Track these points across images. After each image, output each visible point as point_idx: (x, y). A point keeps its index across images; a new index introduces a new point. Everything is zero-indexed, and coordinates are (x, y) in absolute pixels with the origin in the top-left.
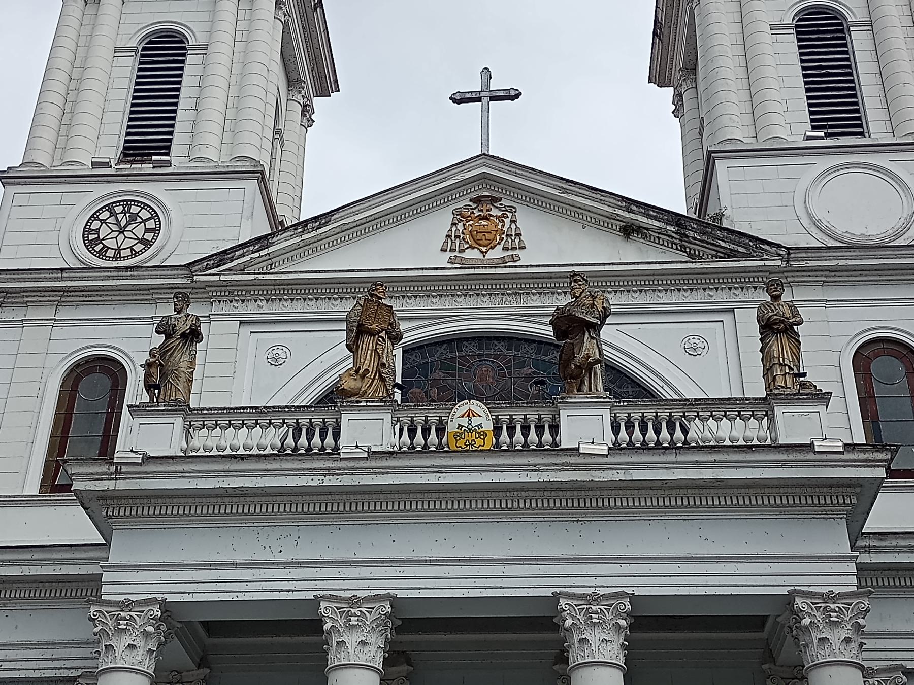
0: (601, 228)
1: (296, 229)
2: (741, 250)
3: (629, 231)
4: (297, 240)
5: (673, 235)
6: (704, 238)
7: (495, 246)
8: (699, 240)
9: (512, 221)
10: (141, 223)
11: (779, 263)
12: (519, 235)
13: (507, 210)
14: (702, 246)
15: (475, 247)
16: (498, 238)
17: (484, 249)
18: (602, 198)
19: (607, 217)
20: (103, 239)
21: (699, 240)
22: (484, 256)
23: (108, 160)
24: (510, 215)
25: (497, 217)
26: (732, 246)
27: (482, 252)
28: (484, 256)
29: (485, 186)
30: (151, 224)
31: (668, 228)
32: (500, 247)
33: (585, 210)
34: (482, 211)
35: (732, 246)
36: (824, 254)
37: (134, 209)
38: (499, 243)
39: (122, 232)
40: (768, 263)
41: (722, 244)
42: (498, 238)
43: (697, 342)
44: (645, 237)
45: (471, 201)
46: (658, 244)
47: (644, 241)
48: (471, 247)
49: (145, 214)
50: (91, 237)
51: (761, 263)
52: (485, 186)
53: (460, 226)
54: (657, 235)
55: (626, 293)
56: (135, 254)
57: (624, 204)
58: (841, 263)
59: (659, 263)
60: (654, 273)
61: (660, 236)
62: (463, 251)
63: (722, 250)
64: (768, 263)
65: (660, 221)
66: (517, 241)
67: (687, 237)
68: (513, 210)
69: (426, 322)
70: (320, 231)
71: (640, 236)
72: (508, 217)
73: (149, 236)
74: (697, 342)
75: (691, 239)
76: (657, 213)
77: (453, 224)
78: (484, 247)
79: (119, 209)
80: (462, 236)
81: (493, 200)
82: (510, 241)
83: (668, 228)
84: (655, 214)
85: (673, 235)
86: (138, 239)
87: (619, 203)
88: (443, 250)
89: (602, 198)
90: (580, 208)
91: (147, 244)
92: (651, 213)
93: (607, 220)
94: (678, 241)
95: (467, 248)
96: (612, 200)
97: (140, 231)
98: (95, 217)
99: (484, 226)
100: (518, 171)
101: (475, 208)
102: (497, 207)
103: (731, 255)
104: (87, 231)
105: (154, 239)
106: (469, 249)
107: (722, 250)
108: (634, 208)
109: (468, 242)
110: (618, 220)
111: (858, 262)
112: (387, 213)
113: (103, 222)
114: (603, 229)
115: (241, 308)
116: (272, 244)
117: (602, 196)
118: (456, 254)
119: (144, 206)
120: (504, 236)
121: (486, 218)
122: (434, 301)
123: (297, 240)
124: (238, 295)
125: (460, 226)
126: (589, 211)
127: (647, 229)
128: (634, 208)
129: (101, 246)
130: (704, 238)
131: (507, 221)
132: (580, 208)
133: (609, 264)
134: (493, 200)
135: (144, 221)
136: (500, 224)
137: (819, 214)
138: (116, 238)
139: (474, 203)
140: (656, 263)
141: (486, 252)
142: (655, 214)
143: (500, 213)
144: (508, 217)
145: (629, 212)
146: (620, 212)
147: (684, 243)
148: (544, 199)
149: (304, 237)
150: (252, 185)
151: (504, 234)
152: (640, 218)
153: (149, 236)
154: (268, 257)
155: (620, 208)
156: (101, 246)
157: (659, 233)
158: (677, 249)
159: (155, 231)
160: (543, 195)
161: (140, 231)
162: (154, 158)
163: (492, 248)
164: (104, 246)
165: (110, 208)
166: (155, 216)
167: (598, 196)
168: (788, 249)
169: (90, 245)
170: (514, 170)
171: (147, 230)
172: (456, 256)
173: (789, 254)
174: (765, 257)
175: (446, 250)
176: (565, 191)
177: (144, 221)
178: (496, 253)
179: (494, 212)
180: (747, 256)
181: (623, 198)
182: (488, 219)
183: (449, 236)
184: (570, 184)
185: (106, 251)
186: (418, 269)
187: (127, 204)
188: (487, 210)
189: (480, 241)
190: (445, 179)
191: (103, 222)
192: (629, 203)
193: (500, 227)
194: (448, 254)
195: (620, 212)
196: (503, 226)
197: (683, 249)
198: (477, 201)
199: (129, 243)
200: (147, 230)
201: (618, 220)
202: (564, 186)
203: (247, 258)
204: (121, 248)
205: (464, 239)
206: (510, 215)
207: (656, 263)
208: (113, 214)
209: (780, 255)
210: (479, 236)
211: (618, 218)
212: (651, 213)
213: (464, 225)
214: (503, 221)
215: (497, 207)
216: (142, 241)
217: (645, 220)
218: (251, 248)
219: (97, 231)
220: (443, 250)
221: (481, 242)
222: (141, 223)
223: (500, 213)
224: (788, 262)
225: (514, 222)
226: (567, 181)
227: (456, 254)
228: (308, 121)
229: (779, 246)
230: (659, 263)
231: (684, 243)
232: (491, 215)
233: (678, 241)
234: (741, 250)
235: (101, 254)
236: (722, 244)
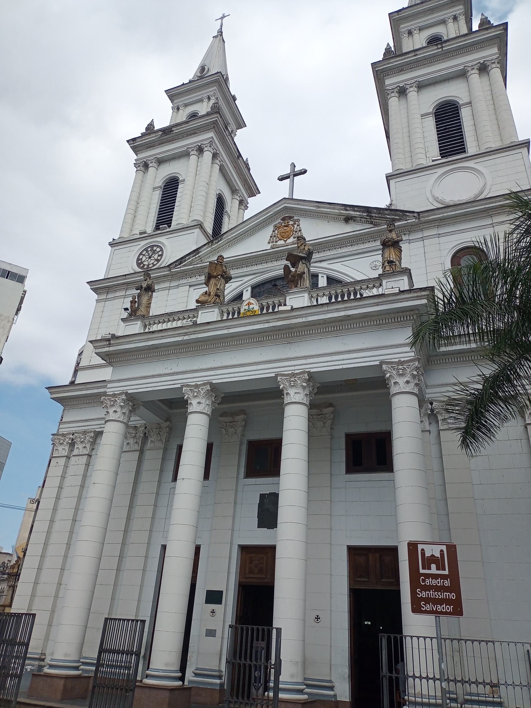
0: (336, 221)
1: (209, 244)
2: (397, 217)
3: (348, 220)
5: (367, 217)
6: (380, 216)
7: (290, 237)
8: (378, 217)
9: (298, 225)
10: (156, 253)
11: (414, 220)
12: (300, 231)
13: (296, 221)
14: (380, 220)
15: (282, 239)
16: (292, 233)
17: (285, 239)
18: (334, 207)
19: (338, 215)
20: (143, 262)
21: (378, 217)
22: (285, 242)
23: (145, 231)
24: (297, 223)
25: (292, 225)
26: (392, 217)
27: (284, 241)
28: (285, 242)
29: (287, 212)
30: (160, 253)
31: (364, 214)
32: (292, 237)
33: (329, 214)
34: (285, 223)
35: (392, 217)
36: (437, 212)
37: (155, 248)
38: (292, 236)
39: (150, 258)
40: (409, 221)
41: (388, 216)
42: (292, 233)
43: (375, 263)
44: (354, 221)
45: (281, 220)
46: (361, 223)
47: (354, 223)
48: (280, 240)
49: (158, 250)
50: (139, 262)
51: (406, 222)
52: (287, 212)
53: (276, 232)
54: (360, 219)
55: (345, 247)
57: (344, 207)
58: (445, 215)
59: (358, 231)
60: (357, 236)
61: (361, 219)
62: (276, 242)
63: (389, 220)
64: (409, 221)
65: (359, 212)
66: (299, 233)
67: (372, 217)
68: (298, 220)
69: (260, 274)
70: (218, 244)
71: (352, 221)
72: (296, 224)
73: (159, 258)
74: (375, 263)
75: (374, 217)
76: (358, 208)
77: (273, 231)
78: (285, 238)
80: (277, 235)
81: (290, 218)
82: (296, 234)
83: (364, 214)
84: (357, 209)
85: (367, 217)
86: (155, 259)
87: (342, 208)
88: (269, 243)
89: (334, 207)
90: (326, 214)
91: (158, 261)
92: (356, 209)
93: (338, 216)
94: (369, 220)
95: (278, 240)
96: (338, 207)
98: (141, 254)
99: (285, 229)
100: (298, 203)
101: (283, 223)
102: (292, 221)
104: (138, 259)
106: (280, 241)
107: (389, 220)
108: (348, 208)
109: (279, 238)
110: (343, 216)
111: (454, 213)
112: (246, 232)
113: (144, 255)
114: (337, 221)
115: (190, 280)
116: (200, 252)
117: (334, 206)
118: (274, 243)
120: (294, 232)
122: (264, 265)
123: (210, 249)
124: (189, 275)
125: (276, 232)
126: (330, 214)
127: (355, 217)
128: (348, 208)
129: (142, 264)
130: (380, 216)
131: (296, 226)
132: (326, 214)
133: (336, 235)
134: (290, 218)
135: (158, 252)
136: (293, 228)
137: (437, 195)
138: (148, 261)
139: (283, 220)
140: (357, 231)
141: (286, 241)
142: (357, 209)
143: (292, 223)
144: (296, 224)
145: (346, 211)
146: (342, 212)
147: (372, 220)
148: (311, 213)
149: (212, 247)
150: (197, 231)
151: (294, 231)
152: (351, 212)
153: (159, 258)
154: (199, 258)
155: (342, 210)
156: (142, 264)
157: (361, 218)
158: (369, 223)
159: (161, 256)
160: (310, 211)
161: (156, 256)
162: (160, 226)
163: (289, 238)
164: (144, 264)
165: (146, 250)
166: (162, 250)
167: (333, 206)
168: (418, 213)
170: (297, 202)
171: (159, 256)
172: (274, 245)
173: (419, 215)
174: (408, 218)
175: (270, 243)
176: (318, 207)
177: (158, 252)
179: (291, 223)
181: (342, 204)
182: (288, 226)
183: (271, 237)
184: (320, 203)
185: (144, 266)
186: (255, 252)
187: (152, 246)
188: (287, 223)
189: (285, 236)
190: (269, 213)
191: (144, 255)
192: (345, 207)
193: (292, 229)
194: (271, 244)
195: (342, 212)
196: (294, 228)
197: (372, 223)
198: (283, 219)
199: (152, 261)
200: (159, 256)
201: (343, 216)
202: (318, 205)
203: (191, 259)
204: (150, 264)
205: (277, 237)
206: (297, 223)
207: (357, 231)
208: (147, 251)
209: (415, 216)
210: (283, 234)
211: (342, 215)
212: (356, 209)
213: (278, 230)
214: (294, 226)
215: (292, 221)
217: (353, 213)
218: (192, 255)
219: (141, 259)
220: (269, 243)
221: (284, 237)
222: (156, 253)
223: (292, 223)
224: (419, 219)
226: (319, 202)
227: (274, 243)
228: (245, 207)
229: (413, 212)
230: (358, 231)
231: (372, 220)
232: (289, 225)
233: (369, 220)
234: (397, 217)
236: (388, 216)
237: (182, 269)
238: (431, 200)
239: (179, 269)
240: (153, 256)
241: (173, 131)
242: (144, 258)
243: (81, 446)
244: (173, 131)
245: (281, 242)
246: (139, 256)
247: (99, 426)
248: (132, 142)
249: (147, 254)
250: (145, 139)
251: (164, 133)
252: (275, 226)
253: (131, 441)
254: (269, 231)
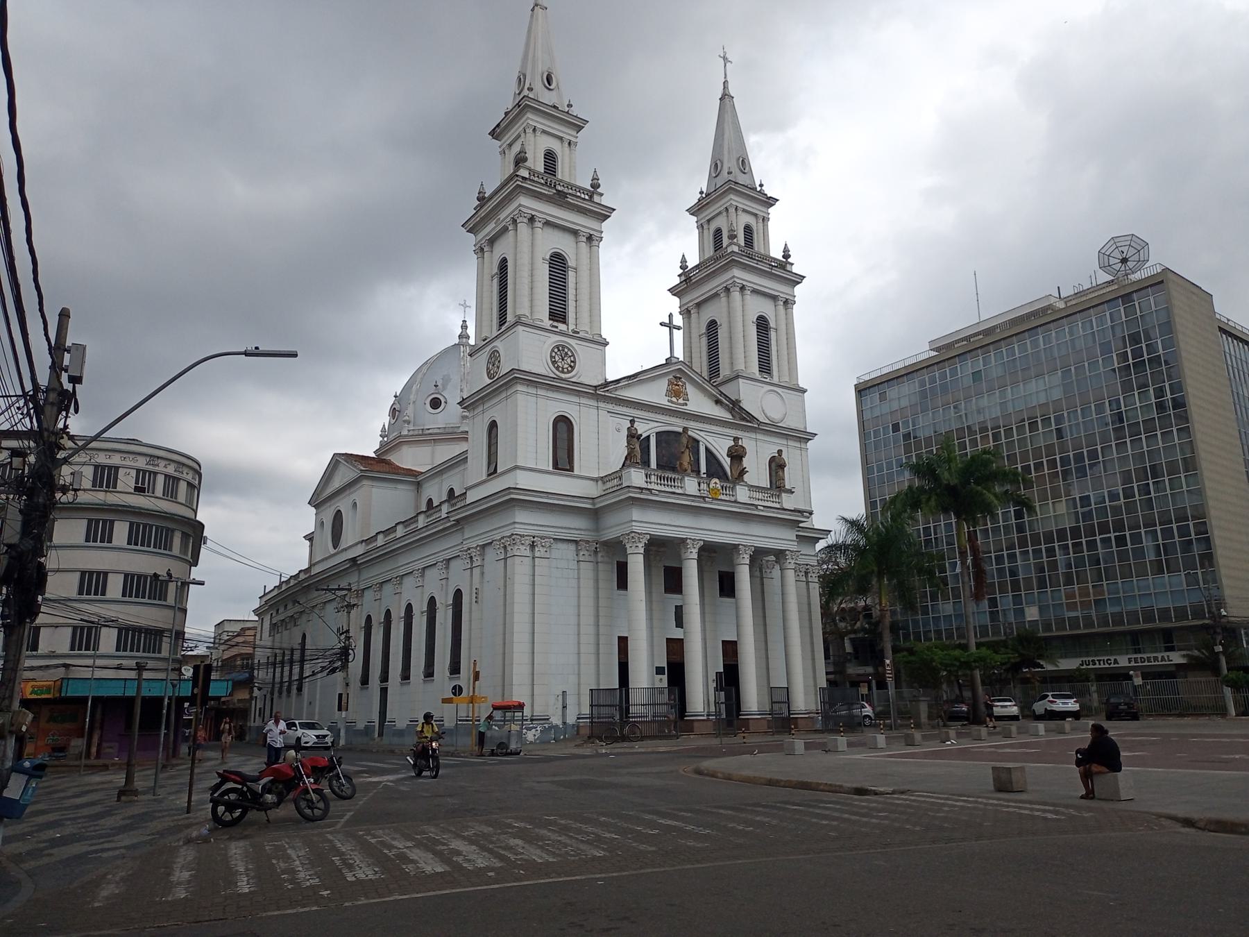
3: (718, 402)
4: (627, 383)
44: (721, 405)
50: (553, 360)
56: (569, 372)
79: (561, 348)
81: (680, 378)
91: (573, 368)
97: (569, 361)
98: (553, 350)
103: (744, 419)
104: (551, 357)
105: (575, 365)
119: (569, 349)
121: (678, 385)
135: (570, 357)
153: (572, 364)
159: (574, 362)
165: (557, 347)
166: (573, 355)
169: (554, 363)
171: (572, 361)
177: (570, 357)
178: (681, 401)
179: (680, 383)
180: (748, 421)
187: (564, 347)
194: (667, 398)
197: (731, 413)
198: (675, 377)
216: (570, 366)
225: (686, 389)
235: (557, 368)
237: (607, 394)
238: (761, 409)
239: (603, 393)
240: (566, 358)
241: (568, 198)
242: (557, 358)
243: (541, 549)
244: (568, 198)
245: (674, 399)
246: (551, 354)
247: (553, 533)
248: (521, 180)
249: (558, 353)
250: (536, 187)
251: (558, 194)
252: (670, 383)
253: (586, 553)
254: (663, 384)
